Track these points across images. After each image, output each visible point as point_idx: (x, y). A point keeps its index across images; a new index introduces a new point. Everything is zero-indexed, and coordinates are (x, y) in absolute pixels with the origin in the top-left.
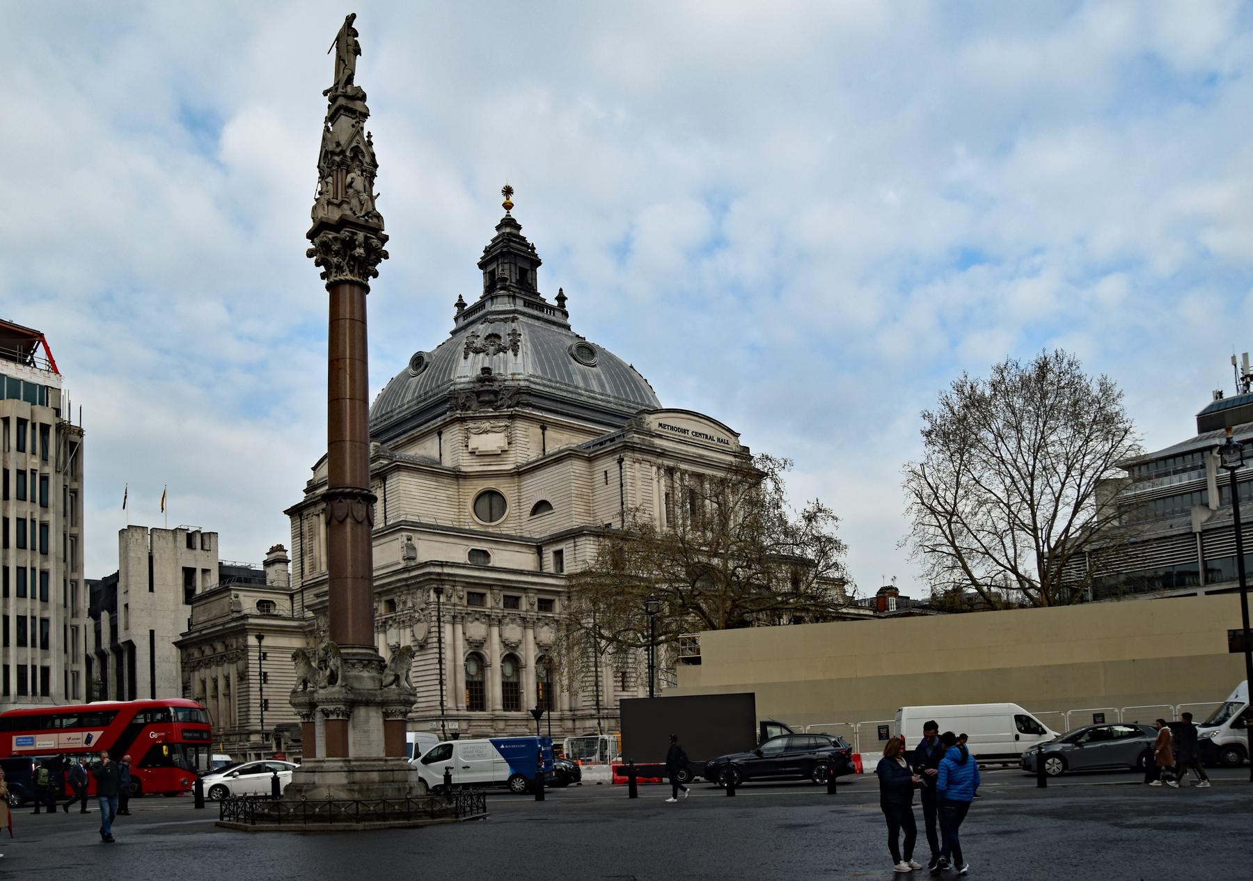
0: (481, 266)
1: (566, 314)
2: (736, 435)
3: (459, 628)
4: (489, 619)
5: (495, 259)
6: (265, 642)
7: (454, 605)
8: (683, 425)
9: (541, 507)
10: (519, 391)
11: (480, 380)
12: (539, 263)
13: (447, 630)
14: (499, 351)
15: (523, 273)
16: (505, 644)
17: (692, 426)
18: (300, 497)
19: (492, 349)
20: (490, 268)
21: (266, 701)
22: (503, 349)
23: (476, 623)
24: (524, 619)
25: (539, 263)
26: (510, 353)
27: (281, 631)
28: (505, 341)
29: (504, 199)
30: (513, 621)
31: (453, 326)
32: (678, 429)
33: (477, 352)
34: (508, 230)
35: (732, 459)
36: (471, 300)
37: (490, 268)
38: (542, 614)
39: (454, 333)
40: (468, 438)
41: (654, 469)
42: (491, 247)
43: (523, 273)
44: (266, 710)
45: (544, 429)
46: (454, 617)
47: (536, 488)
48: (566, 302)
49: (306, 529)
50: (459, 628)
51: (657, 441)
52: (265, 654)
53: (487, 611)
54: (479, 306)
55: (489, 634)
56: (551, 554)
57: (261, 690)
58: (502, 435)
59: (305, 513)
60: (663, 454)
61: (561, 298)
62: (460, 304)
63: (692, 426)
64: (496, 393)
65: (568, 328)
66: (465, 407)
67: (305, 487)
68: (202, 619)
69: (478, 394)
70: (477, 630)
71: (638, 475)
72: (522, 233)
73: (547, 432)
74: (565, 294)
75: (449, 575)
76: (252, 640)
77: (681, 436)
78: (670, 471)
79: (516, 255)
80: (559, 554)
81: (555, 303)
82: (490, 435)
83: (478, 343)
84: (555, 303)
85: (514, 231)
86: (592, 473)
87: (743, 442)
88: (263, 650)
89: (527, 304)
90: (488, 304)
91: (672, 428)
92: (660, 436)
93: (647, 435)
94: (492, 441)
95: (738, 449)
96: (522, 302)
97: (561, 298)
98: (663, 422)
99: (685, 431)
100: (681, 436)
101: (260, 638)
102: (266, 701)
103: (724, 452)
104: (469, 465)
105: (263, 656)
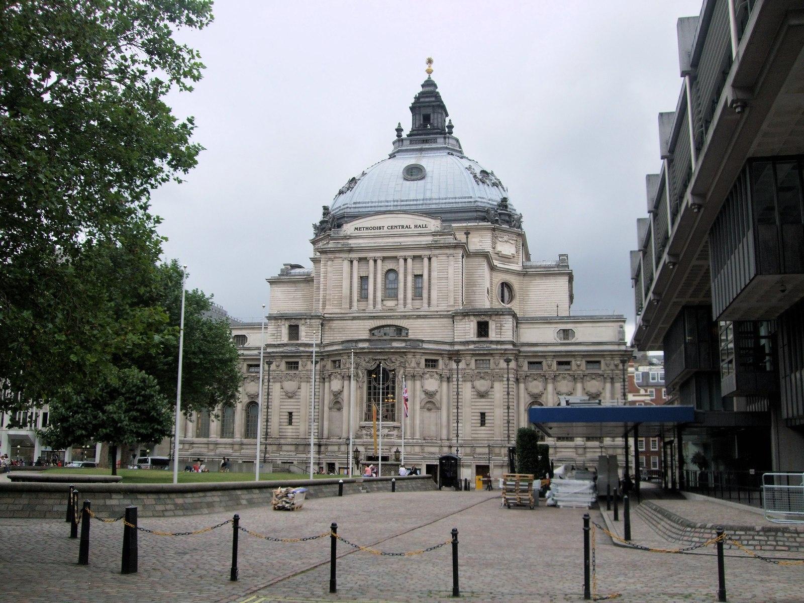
11: (324, 214)
15: (427, 118)
29: (427, 67)
32: (374, 228)
35: (430, 238)
43: (427, 118)
48: (453, 130)
51: (350, 241)
60: (351, 250)
77: (377, 232)
79: (419, 107)
91: (367, 228)
92: (355, 237)
93: (342, 239)
96: (408, 142)
97: (451, 127)
98: (358, 226)
100: (377, 232)
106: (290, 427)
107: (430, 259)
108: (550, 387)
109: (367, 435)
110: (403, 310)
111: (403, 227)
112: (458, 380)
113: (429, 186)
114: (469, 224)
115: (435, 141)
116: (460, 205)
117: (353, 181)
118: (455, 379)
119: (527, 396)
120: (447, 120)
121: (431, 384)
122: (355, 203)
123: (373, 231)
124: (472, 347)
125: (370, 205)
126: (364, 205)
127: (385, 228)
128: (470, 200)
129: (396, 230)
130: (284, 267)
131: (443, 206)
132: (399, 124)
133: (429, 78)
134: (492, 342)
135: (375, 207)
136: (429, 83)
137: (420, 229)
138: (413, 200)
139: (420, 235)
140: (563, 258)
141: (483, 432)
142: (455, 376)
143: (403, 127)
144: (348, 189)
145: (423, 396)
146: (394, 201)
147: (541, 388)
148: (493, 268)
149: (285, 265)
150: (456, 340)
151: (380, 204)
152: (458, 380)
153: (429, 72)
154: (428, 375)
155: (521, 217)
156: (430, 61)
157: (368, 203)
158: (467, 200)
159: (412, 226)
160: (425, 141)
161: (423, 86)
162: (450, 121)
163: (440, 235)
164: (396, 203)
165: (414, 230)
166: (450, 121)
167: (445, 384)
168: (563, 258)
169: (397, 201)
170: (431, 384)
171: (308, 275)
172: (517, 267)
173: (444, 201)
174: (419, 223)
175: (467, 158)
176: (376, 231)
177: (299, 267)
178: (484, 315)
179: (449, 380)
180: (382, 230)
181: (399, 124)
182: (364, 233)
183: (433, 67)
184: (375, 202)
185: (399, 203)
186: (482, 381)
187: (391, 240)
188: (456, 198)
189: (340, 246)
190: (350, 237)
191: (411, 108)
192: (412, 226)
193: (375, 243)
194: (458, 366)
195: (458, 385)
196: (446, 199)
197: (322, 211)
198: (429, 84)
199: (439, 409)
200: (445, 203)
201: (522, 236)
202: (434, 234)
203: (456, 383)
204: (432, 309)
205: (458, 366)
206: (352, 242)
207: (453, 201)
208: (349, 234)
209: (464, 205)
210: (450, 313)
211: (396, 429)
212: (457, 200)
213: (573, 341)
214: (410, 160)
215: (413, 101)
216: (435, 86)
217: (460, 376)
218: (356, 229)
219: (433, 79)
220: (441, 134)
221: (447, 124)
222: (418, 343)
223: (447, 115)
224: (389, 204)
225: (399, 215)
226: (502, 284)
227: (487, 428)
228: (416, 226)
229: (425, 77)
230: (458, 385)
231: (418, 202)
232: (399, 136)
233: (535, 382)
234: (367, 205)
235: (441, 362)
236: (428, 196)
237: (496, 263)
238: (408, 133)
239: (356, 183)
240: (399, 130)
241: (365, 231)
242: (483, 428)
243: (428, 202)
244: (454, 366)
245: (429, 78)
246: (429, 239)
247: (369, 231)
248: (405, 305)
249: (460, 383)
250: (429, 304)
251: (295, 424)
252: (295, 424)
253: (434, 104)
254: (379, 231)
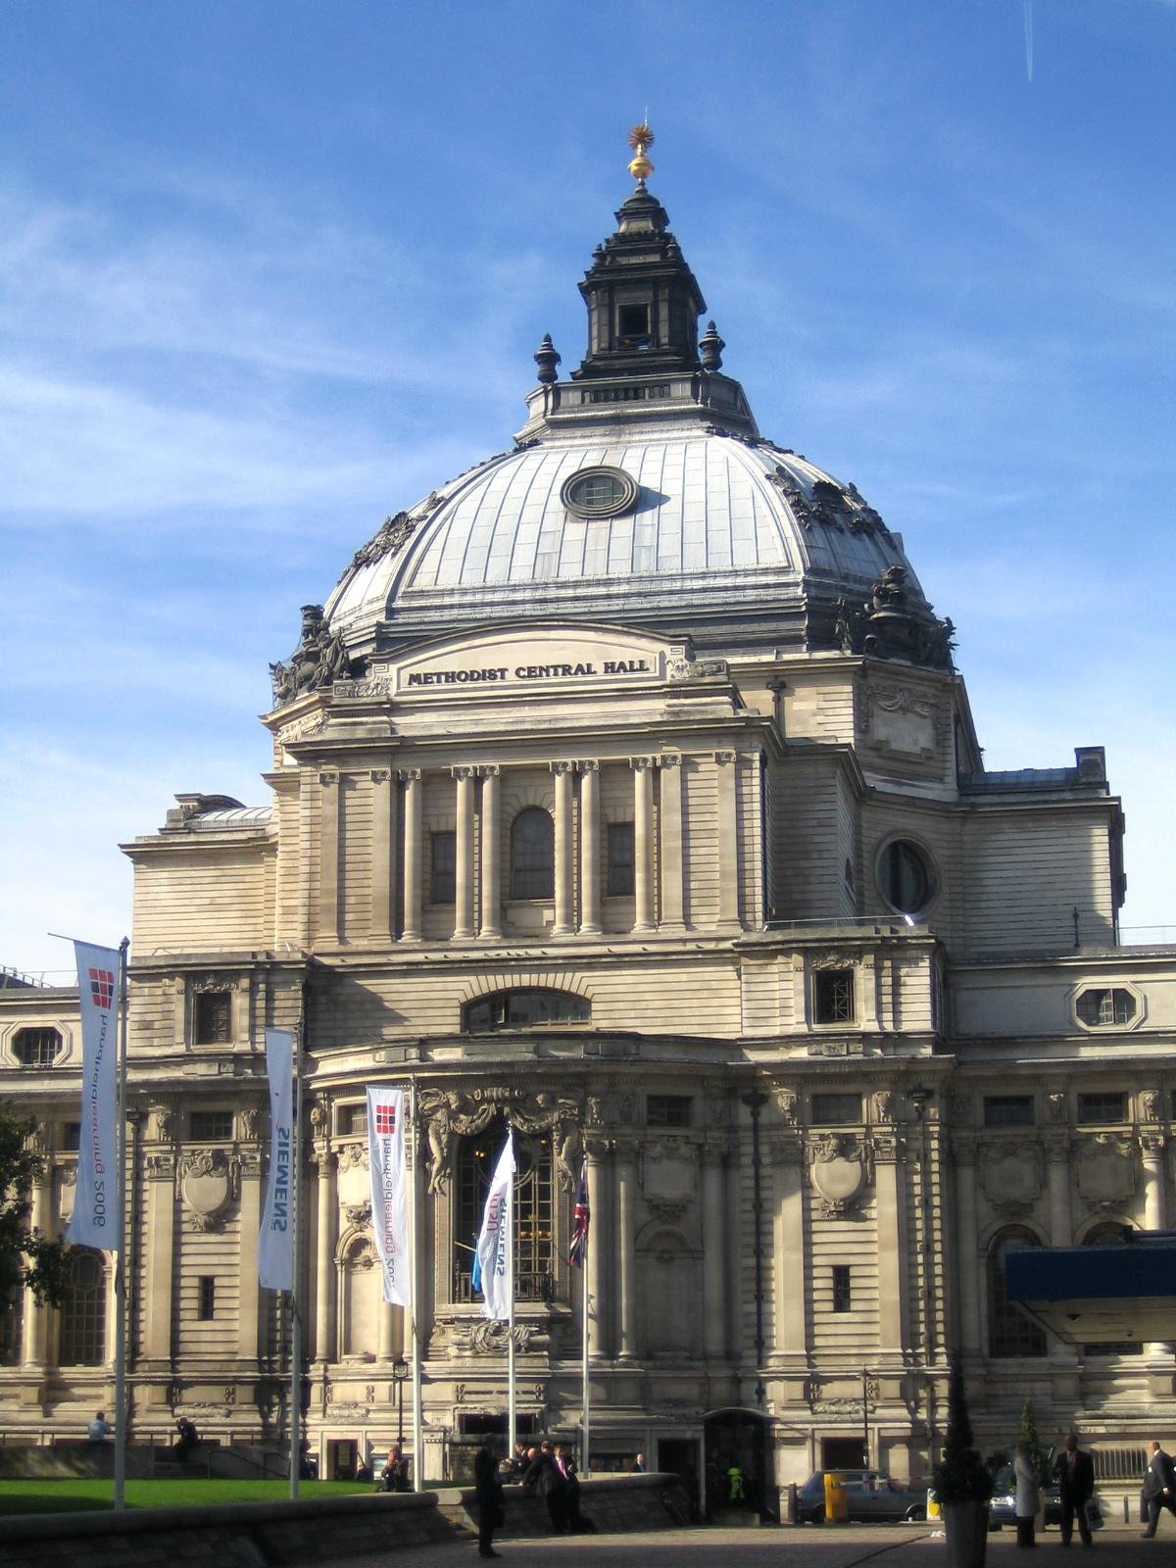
11: (307, 632)
15: (634, 322)
32: (471, 676)
35: (660, 705)
48: (724, 355)
60: (402, 748)
77: (483, 689)
85: (647, 225)
91: (451, 677)
97: (716, 346)
99: (490, 674)
106: (206, 1325)
107: (655, 772)
108: (1057, 1177)
109: (460, 1345)
110: (570, 938)
111: (566, 669)
112: (757, 1163)
113: (647, 537)
114: (786, 657)
115: (662, 390)
116: (751, 595)
117: (400, 523)
118: (747, 1160)
119: (984, 1208)
120: (702, 322)
121: (671, 1180)
122: (407, 595)
123: (469, 684)
124: (802, 1053)
125: (455, 600)
126: (437, 602)
127: (510, 676)
128: (783, 579)
129: (544, 680)
130: (176, 805)
131: (697, 599)
132: (548, 338)
134: (866, 1038)
135: (473, 605)
136: (646, 207)
137: (622, 675)
138: (598, 583)
139: (625, 695)
140: (1091, 761)
141: (837, 1331)
142: (750, 1149)
143: (558, 348)
144: (385, 550)
145: (644, 1216)
146: (535, 587)
147: (1029, 1181)
148: (862, 796)
149: (180, 797)
150: (749, 1032)
151: (489, 598)
152: (757, 1163)
154: (658, 1149)
155: (949, 629)
157: (452, 592)
158: (771, 579)
159: (599, 667)
160: (634, 393)
161: (620, 216)
162: (712, 325)
163: (688, 695)
164: (539, 594)
166: (712, 325)
167: (713, 1180)
168: (1091, 761)
169: (546, 586)
170: (671, 1180)
171: (259, 827)
172: (943, 791)
173: (699, 584)
174: (619, 656)
175: (771, 444)
176: (481, 684)
177: (227, 803)
178: (838, 950)
179: (728, 1163)
180: (498, 682)
181: (548, 338)
182: (440, 691)
184: (474, 591)
185: (552, 593)
186: (840, 1163)
187: (527, 712)
188: (735, 573)
189: (361, 733)
190: (394, 708)
191: (585, 290)
192: (599, 667)
193: (476, 722)
194: (755, 1115)
195: (757, 1178)
196: (704, 576)
197: (299, 622)
198: (646, 207)
199: (697, 1255)
200: (704, 590)
201: (956, 691)
202: (674, 691)
203: (751, 1172)
204: (664, 932)
205: (755, 1115)
206: (410, 725)
207: (729, 582)
209: (763, 594)
210: (728, 945)
211: (558, 1328)
212: (740, 581)
213: (1129, 1027)
214: (581, 453)
215: (590, 263)
216: (659, 216)
217: (764, 1149)
218: (414, 678)
219: (651, 192)
220: (682, 368)
221: (702, 337)
222: (622, 1042)
223: (701, 308)
224: (519, 596)
225: (553, 634)
226: (895, 847)
227: (857, 1318)
228: (609, 667)
229: (631, 192)
230: (757, 1178)
231: (614, 590)
232: (549, 376)
233: (1010, 1164)
234: (447, 601)
235: (700, 1110)
236: (645, 566)
237: (872, 780)
238: (577, 367)
239: (411, 529)
240: (549, 360)
241: (444, 686)
242: (843, 1316)
243: (646, 587)
244: (744, 1116)
246: (654, 710)
247: (458, 685)
248: (572, 920)
249: (764, 1172)
250: (654, 918)
251: (225, 1315)
252: (225, 1315)
253: (659, 273)
254: (488, 683)
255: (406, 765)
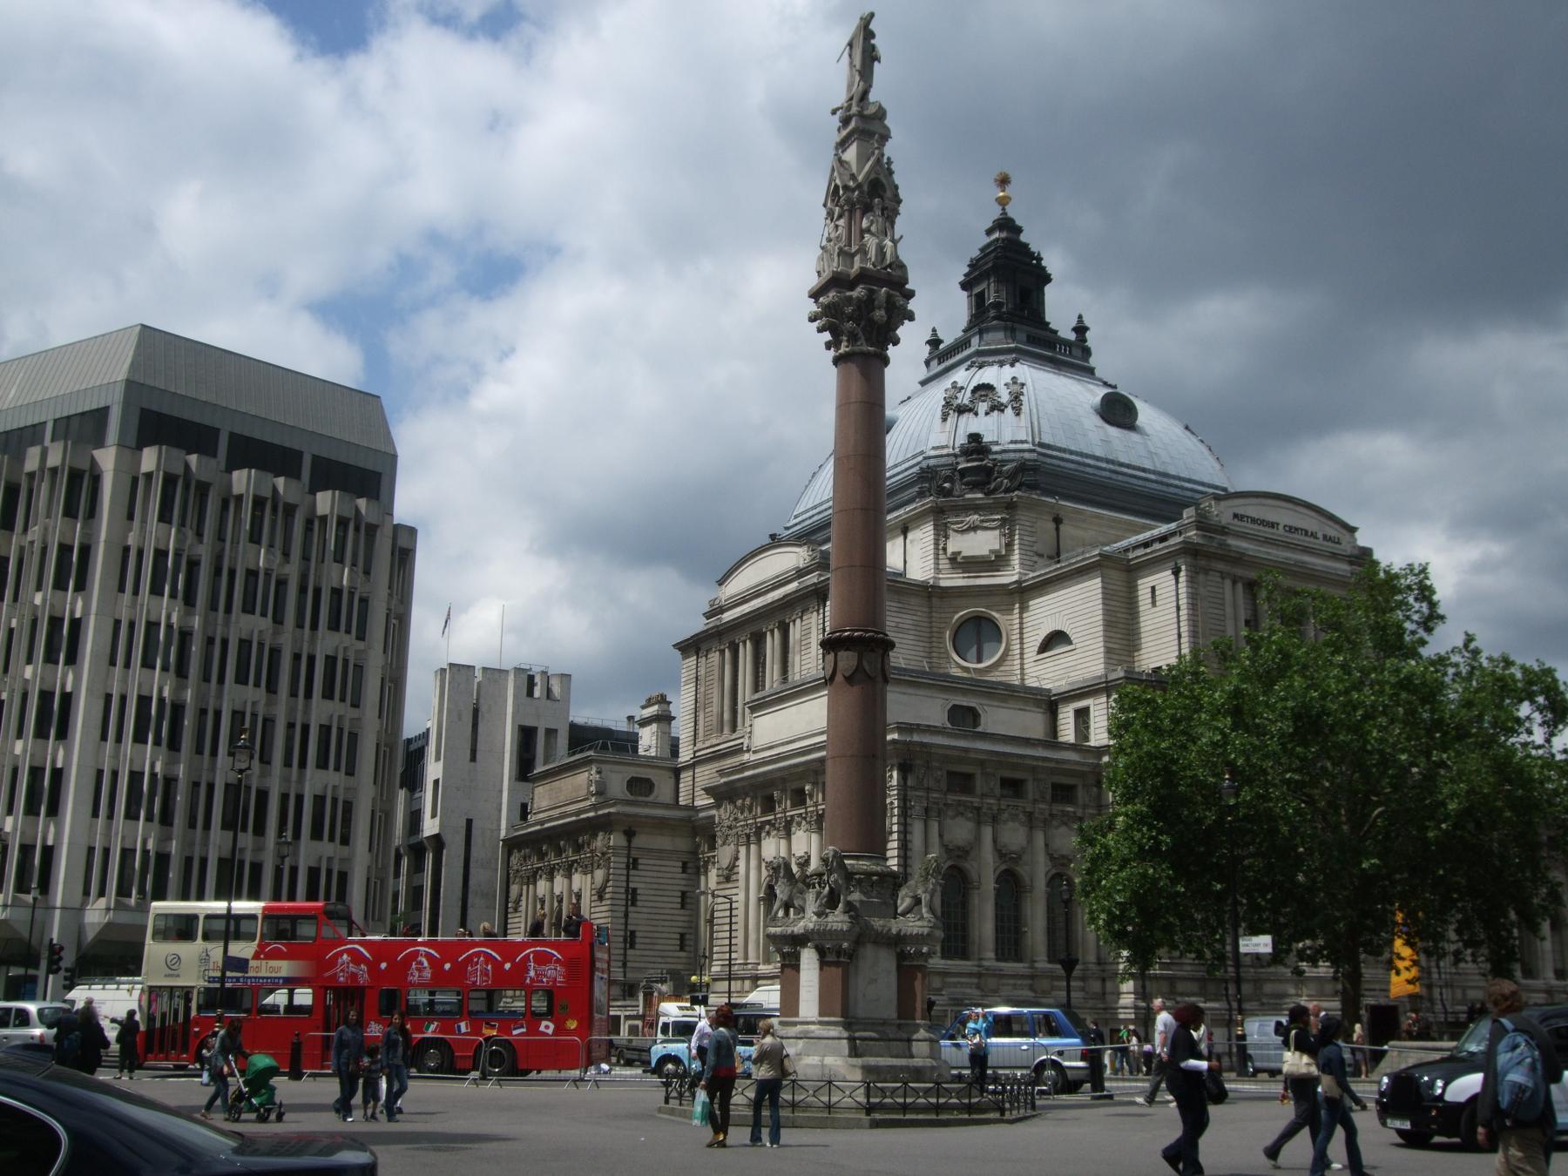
0: (965, 286)
1: (1087, 352)
2: (1353, 530)
3: (934, 827)
4: (979, 817)
5: (984, 276)
6: (640, 841)
7: (928, 790)
8: (1270, 516)
9: (1056, 639)
10: (1024, 468)
11: (966, 452)
12: (1047, 279)
13: (917, 828)
14: (993, 408)
16: (1001, 853)
17: (1284, 517)
18: (699, 625)
19: (983, 407)
20: (977, 290)
21: (633, 933)
22: (998, 407)
23: (960, 820)
24: (1030, 815)
25: (1047, 279)
26: (1009, 411)
27: (661, 825)
28: (1004, 396)
30: (1014, 818)
31: (923, 373)
32: (1263, 523)
33: (961, 410)
34: (1004, 235)
36: (948, 338)
37: (977, 290)
38: (1057, 808)
39: (923, 383)
40: (947, 537)
41: (1228, 583)
42: (978, 260)
44: (632, 946)
45: (1058, 521)
46: (927, 810)
47: (1046, 613)
48: (1088, 334)
49: (702, 672)
50: (934, 827)
52: (635, 860)
53: (976, 801)
54: (962, 344)
55: (978, 838)
56: (1072, 714)
57: (626, 916)
58: (997, 532)
59: (704, 647)
60: (1239, 559)
61: (1081, 330)
62: (934, 342)
63: (1284, 517)
64: (988, 472)
65: (1090, 372)
66: (942, 492)
67: (707, 609)
68: (545, 804)
69: (963, 472)
70: (960, 831)
71: (1202, 590)
72: (1023, 238)
73: (1062, 527)
74: (1087, 323)
75: (923, 745)
76: (616, 839)
78: (1251, 587)
80: (1082, 715)
81: (1072, 336)
82: (981, 535)
83: (964, 398)
84: (1072, 336)
86: (1132, 590)
87: (1362, 540)
88: (634, 853)
89: (1031, 340)
90: (975, 341)
91: (1254, 521)
92: (1238, 535)
93: (1215, 531)
94: (983, 543)
95: (1356, 552)
96: (1023, 337)
97: (1081, 330)
98: (1241, 511)
99: (1273, 525)
101: (630, 834)
102: (633, 933)
103: (1334, 556)
104: (953, 580)
105: (633, 864)
122: (1041, 445)
133: (1004, 213)
136: (1005, 224)
153: (1003, 202)
156: (1004, 181)
159: (1320, 535)
165: (1319, 543)
183: (1010, 191)
198: (1005, 224)
208: (1224, 522)
218: (1236, 516)
228: (1325, 537)
229: (996, 213)
245: (1004, 213)
255: (1239, 572)
